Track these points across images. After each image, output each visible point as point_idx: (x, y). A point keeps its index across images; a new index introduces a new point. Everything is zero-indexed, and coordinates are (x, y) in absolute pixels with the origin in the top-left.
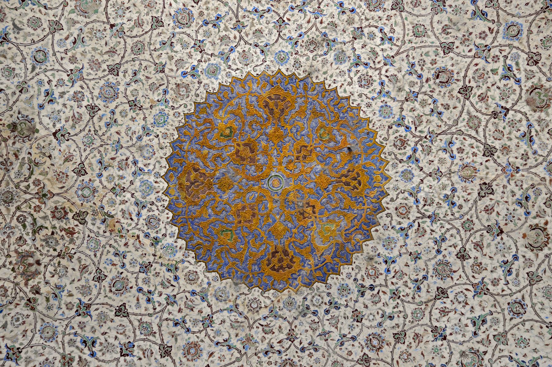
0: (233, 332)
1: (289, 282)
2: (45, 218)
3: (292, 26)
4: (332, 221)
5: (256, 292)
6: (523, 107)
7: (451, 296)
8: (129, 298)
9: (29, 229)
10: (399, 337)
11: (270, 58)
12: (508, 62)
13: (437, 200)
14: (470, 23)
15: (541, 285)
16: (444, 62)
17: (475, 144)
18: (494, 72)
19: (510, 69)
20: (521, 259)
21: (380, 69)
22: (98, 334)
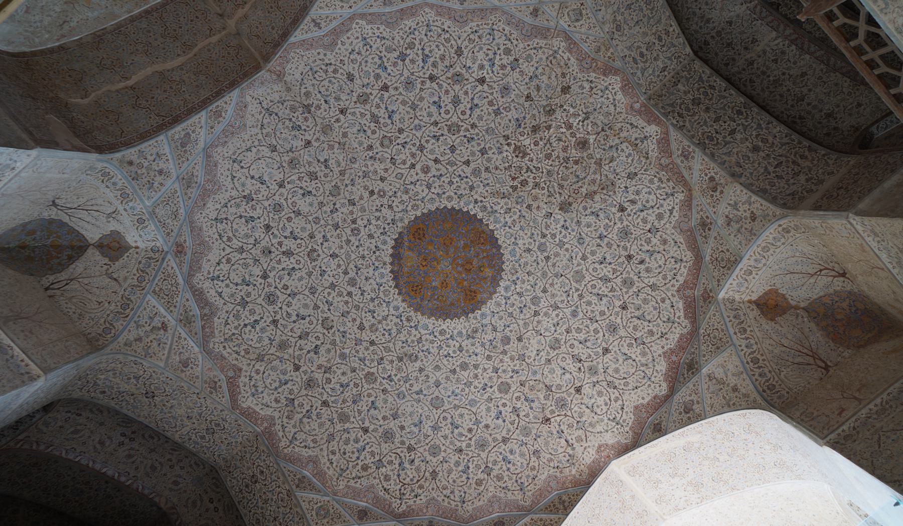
0: (415, 190)
1: (408, 228)
2: (529, 177)
3: (489, 332)
5: (419, 214)
6: (374, 370)
8: (468, 170)
9: (531, 167)
11: (488, 312)
15: (312, 307)
16: (418, 364)
19: (391, 381)
22: (470, 146)
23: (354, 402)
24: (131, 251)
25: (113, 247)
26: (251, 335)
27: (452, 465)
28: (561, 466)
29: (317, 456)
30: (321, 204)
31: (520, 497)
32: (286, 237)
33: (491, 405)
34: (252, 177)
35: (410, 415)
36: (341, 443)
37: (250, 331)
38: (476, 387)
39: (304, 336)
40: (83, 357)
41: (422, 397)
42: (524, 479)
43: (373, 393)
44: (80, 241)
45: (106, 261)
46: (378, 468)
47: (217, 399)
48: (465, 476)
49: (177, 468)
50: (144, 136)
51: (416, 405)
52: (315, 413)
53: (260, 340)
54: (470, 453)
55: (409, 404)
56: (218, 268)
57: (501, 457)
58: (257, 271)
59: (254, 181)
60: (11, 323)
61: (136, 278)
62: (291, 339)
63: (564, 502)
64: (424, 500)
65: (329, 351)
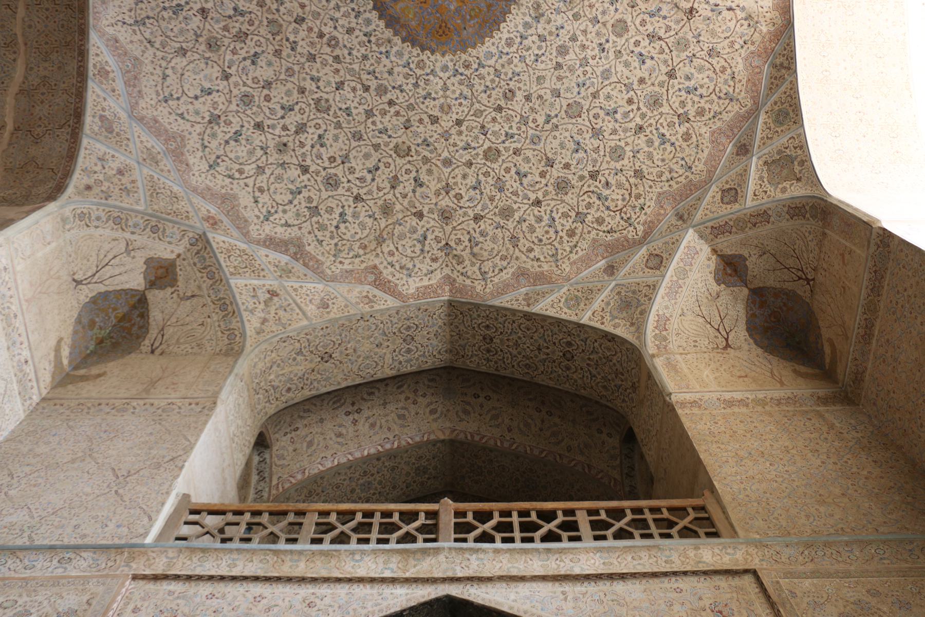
4: (415, 15)
7: (364, 95)
10: (337, 59)
12: (516, 136)
13: (428, 87)
14: (543, 113)
15: (373, 151)
16: (519, 96)
17: (464, 114)
18: (511, 128)
19: (512, 137)
20: (389, 140)
21: (517, 52)
23: (501, 190)
24: (178, 263)
25: (162, 274)
26: (351, 230)
27: (646, 149)
28: (746, 38)
29: (519, 268)
30: (277, 53)
31: (736, 108)
32: (283, 117)
33: (625, 57)
34: (196, 98)
35: (563, 148)
36: (528, 235)
37: (346, 228)
38: (594, 58)
39: (394, 182)
40: (233, 367)
41: (554, 120)
42: (725, 89)
43: (509, 165)
44: (133, 296)
45: (170, 290)
46: (583, 222)
47: (382, 307)
48: (668, 146)
49: (420, 399)
50: (71, 155)
51: (557, 134)
52: (477, 235)
53: (363, 226)
54: (652, 121)
55: (550, 139)
56: (260, 205)
57: (683, 93)
58: (294, 172)
59: (201, 100)
60: (152, 390)
61: (205, 279)
62: (387, 197)
63: (782, 64)
64: (652, 204)
65: (430, 172)
